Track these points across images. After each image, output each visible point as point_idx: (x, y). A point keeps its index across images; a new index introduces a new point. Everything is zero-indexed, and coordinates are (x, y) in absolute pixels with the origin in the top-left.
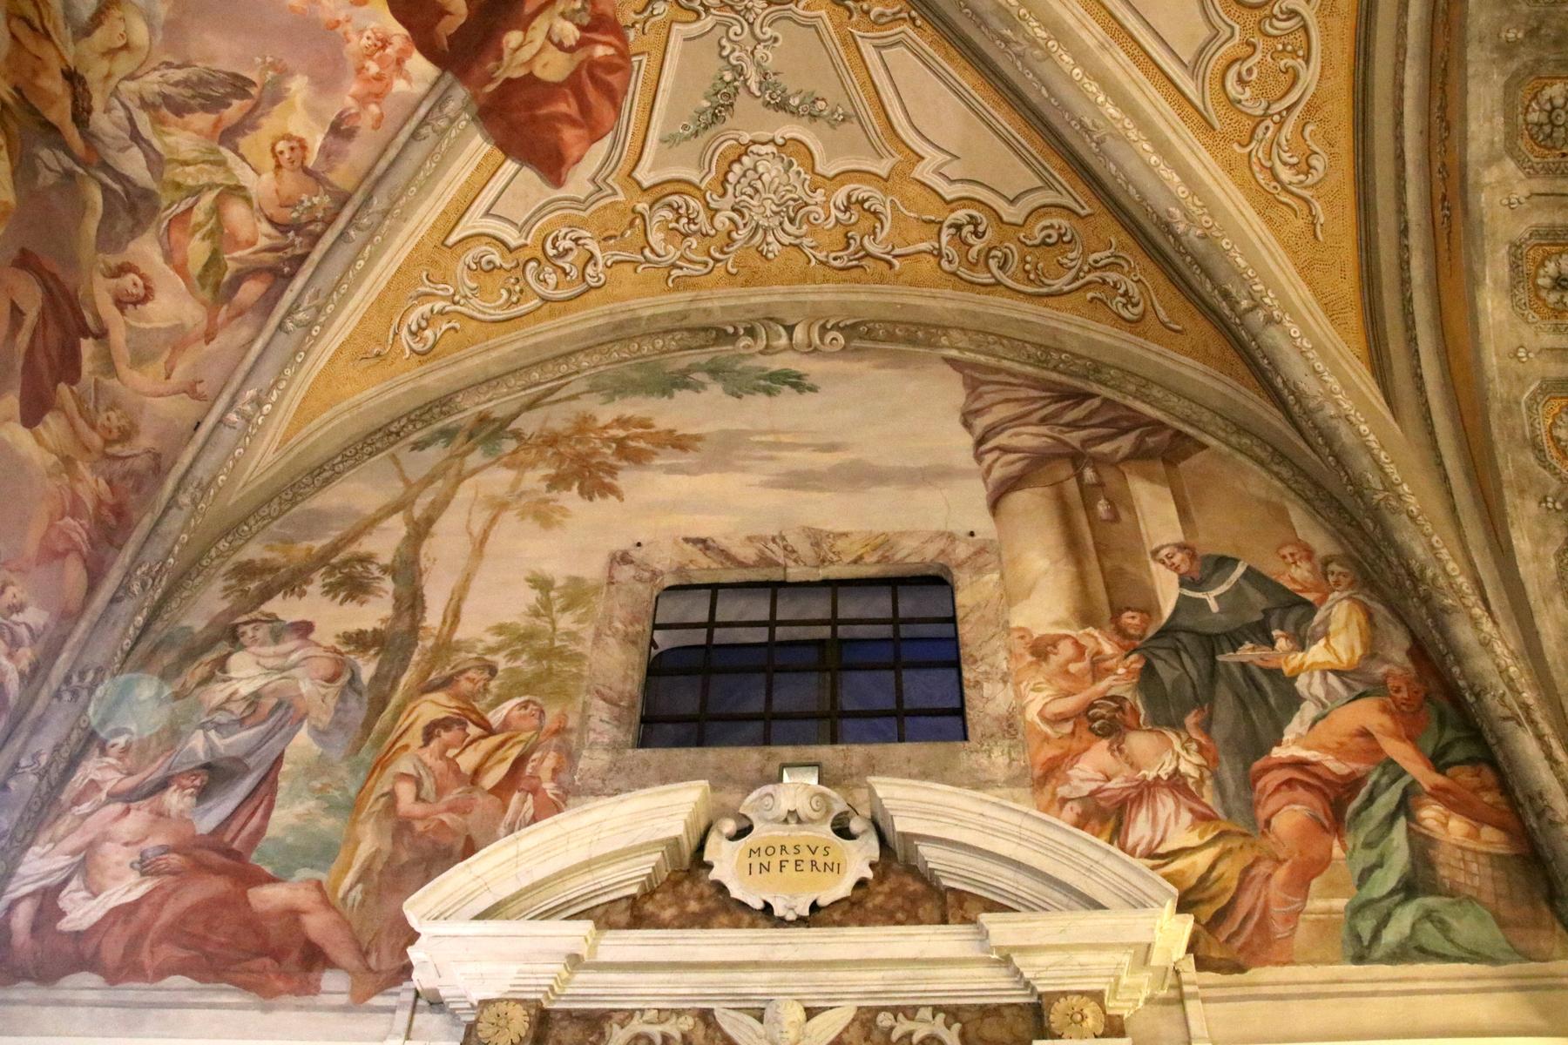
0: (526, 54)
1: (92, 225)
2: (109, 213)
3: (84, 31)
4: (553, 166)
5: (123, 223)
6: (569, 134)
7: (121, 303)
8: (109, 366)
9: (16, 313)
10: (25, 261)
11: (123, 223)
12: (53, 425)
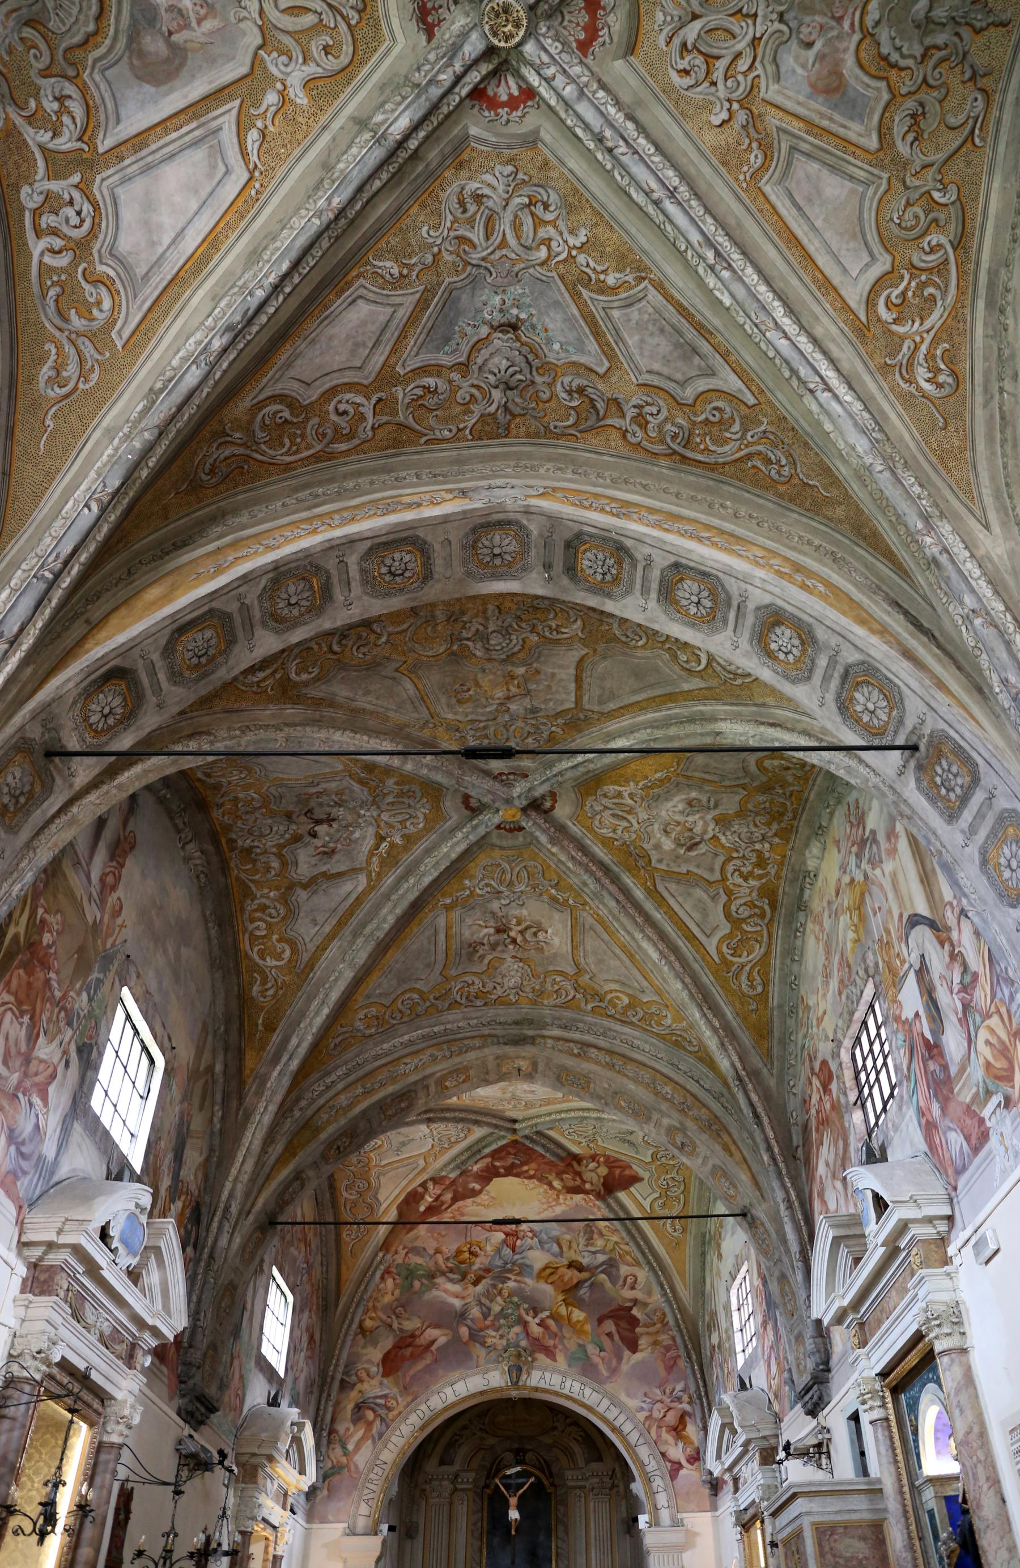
0: (595, 1179)
1: (608, 1285)
2: (609, 1275)
3: (561, 1254)
4: (636, 1179)
5: (614, 1271)
6: (627, 1172)
7: (633, 1288)
8: (645, 1305)
9: (609, 1335)
10: (600, 1321)
11: (614, 1271)
12: (643, 1342)
